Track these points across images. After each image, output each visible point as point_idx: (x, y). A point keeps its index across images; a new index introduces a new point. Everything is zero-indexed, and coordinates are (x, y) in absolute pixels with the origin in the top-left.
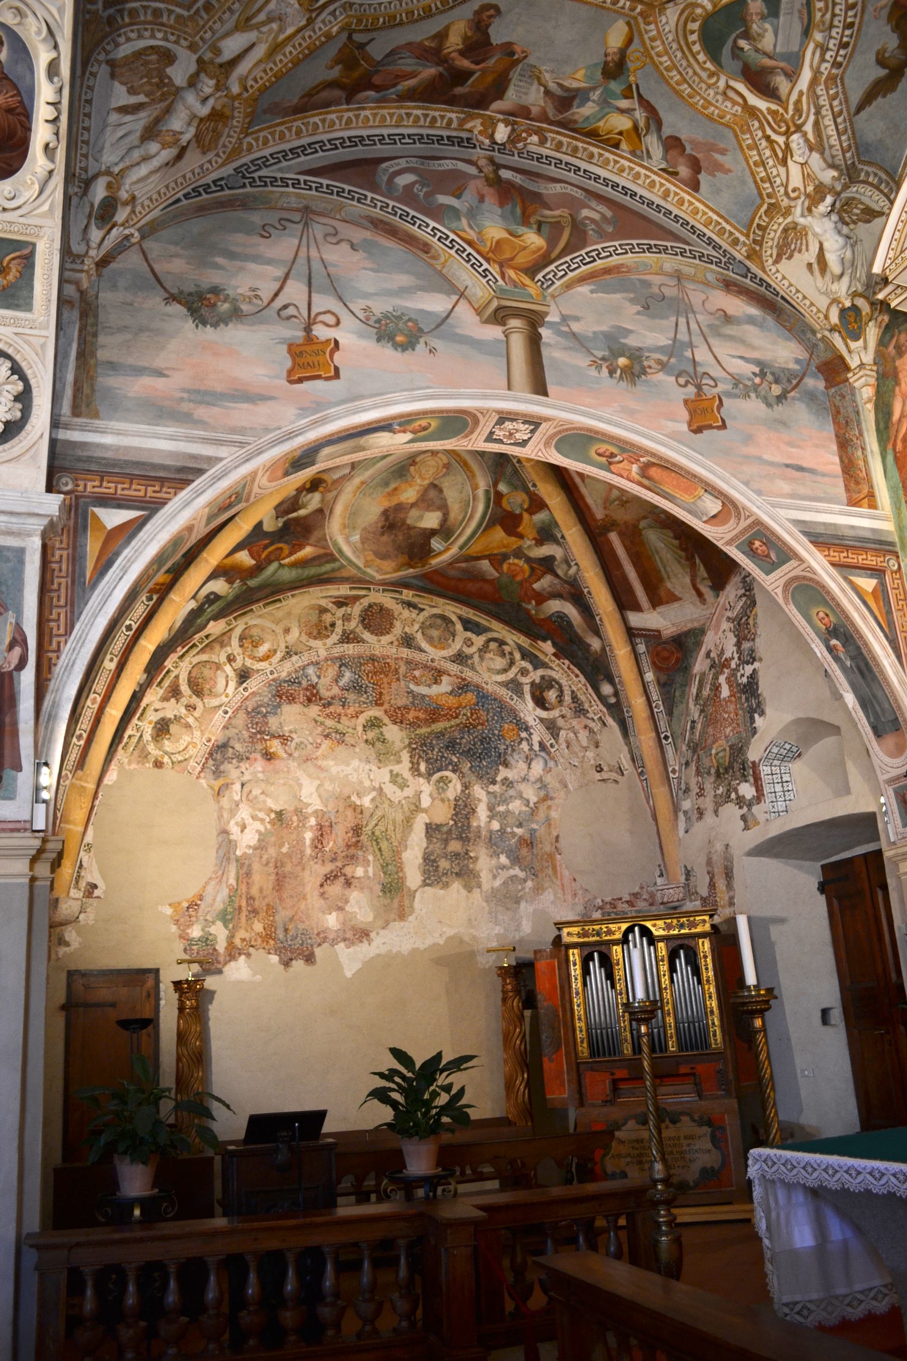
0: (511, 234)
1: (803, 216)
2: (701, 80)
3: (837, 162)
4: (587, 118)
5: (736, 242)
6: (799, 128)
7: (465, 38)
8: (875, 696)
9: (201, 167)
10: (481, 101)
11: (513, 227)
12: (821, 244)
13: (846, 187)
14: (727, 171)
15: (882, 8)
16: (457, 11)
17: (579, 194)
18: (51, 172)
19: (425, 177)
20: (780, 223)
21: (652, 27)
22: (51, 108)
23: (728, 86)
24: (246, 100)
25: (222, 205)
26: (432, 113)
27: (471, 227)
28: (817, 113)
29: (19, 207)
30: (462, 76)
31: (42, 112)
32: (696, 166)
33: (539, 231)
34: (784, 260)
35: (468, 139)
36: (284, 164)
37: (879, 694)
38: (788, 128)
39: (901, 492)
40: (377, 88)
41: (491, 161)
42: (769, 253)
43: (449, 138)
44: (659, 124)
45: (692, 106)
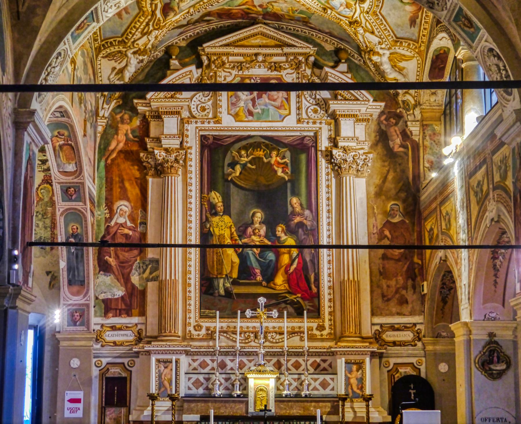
8: (78, 268)
12: (127, 65)
34: (106, 59)
37: (81, 268)
39: (104, 181)
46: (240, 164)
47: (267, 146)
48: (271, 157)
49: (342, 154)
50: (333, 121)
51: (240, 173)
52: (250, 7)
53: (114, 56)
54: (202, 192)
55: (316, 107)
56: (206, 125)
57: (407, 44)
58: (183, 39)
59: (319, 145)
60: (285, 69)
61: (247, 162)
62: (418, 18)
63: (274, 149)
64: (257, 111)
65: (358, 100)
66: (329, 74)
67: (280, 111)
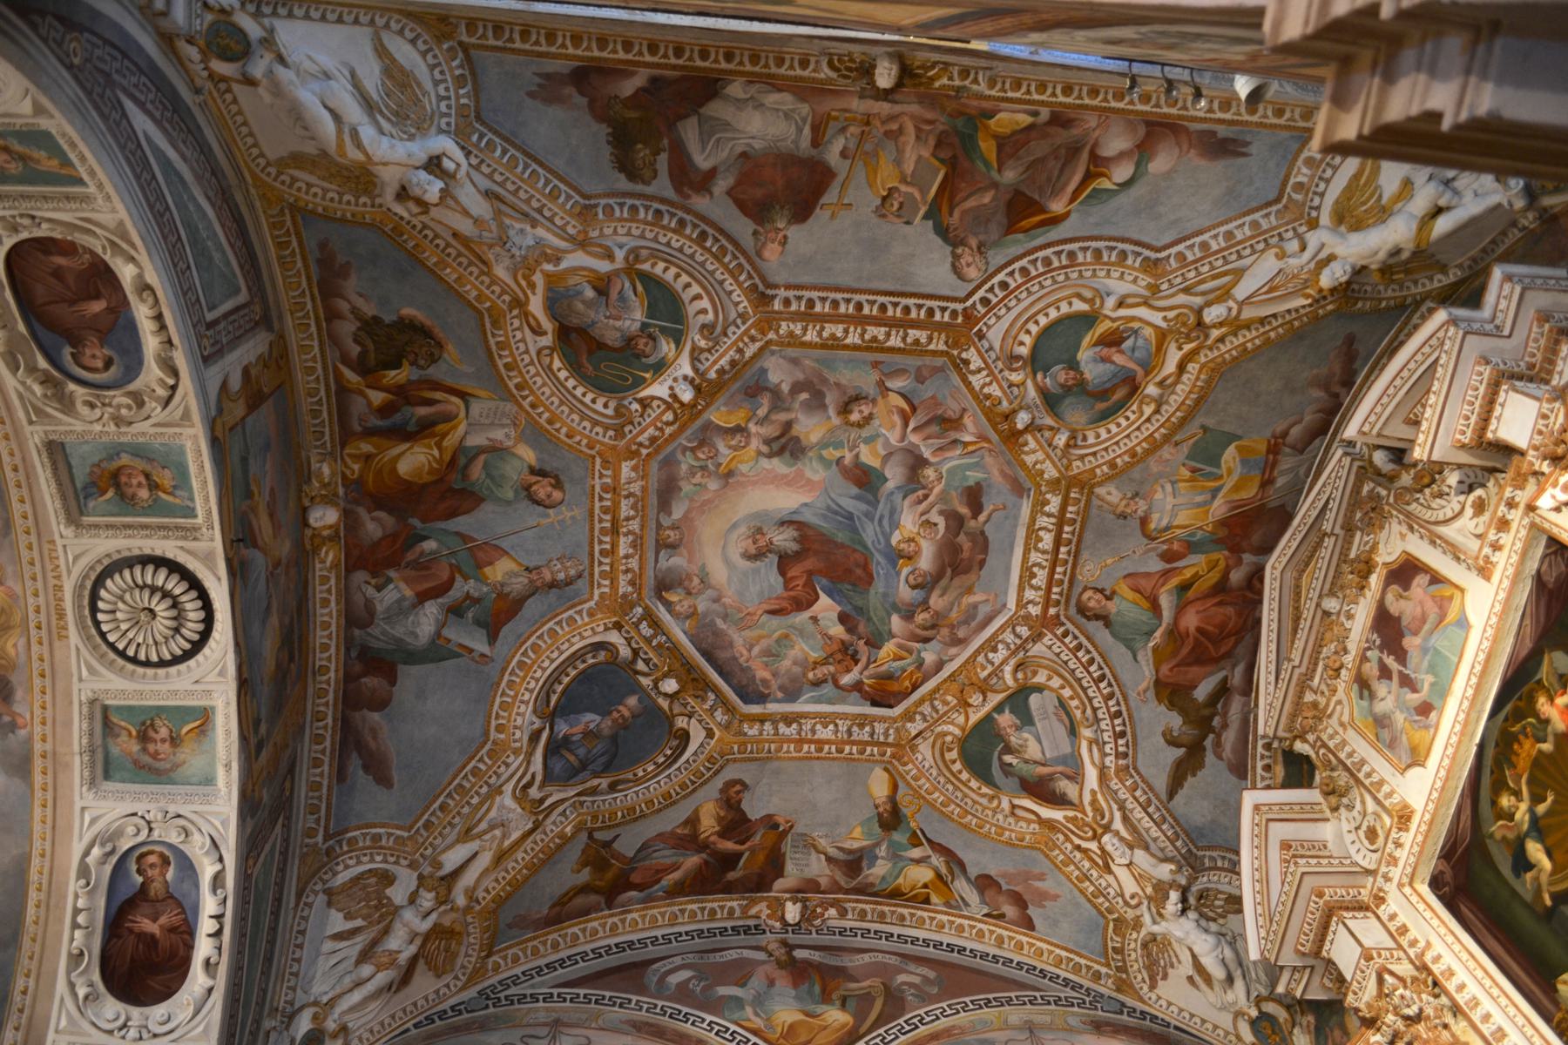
0: (807, 1015)
1: (1155, 922)
2: (985, 808)
3: (1170, 855)
4: (883, 878)
5: (1097, 976)
6: (1107, 828)
7: (720, 819)
9: (437, 992)
10: (760, 883)
11: (811, 1008)
12: (1191, 950)
13: (1192, 880)
14: (1055, 897)
15: (1145, 691)
16: (700, 794)
17: (893, 960)
18: (210, 990)
19: (701, 972)
20: (1134, 940)
21: (910, 766)
22: (214, 921)
23: (1014, 806)
24: (480, 912)
25: (456, 1030)
26: (709, 905)
27: (757, 1015)
28: (1122, 808)
29: (171, 1031)
30: (730, 860)
31: (206, 926)
32: (1020, 901)
33: (843, 1006)
34: (1160, 983)
35: (756, 927)
36: (537, 979)
38: (1095, 831)
40: (640, 887)
41: (784, 943)
42: (1139, 978)
43: (733, 928)
44: (962, 866)
45: (987, 836)
46: (1527, 835)
47: (1518, 715)
48: (1547, 721)
51: (1549, 854)
52: (1175, 581)
53: (1156, 963)
54: (1548, 1019)
55: (1472, 497)
56: (1402, 854)
57: (1305, 170)
58: (1267, 768)
60: (1376, 544)
61: (1531, 811)
62: (1214, 133)
63: (1531, 700)
64: (1426, 687)
65: (1437, 360)
66: (1366, 429)
67: (1447, 620)
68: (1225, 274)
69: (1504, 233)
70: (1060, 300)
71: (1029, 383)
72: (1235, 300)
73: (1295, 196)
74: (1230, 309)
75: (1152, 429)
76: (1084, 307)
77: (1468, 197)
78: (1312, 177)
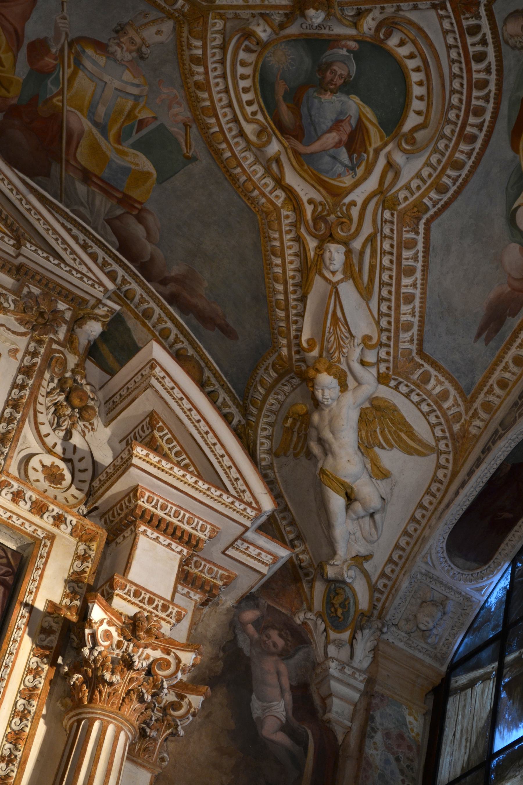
49: (116, 637)
50: (103, 534)
55: (62, 465)
57: (438, 389)
59: (28, 585)
65: (227, 491)
66: (158, 369)
68: (371, 280)
69: (293, 523)
70: (429, 106)
71: (352, 32)
72: (341, 281)
73: (419, 372)
74: (333, 273)
75: (223, 121)
76: (407, 127)
77: (351, 526)
78: (429, 394)
